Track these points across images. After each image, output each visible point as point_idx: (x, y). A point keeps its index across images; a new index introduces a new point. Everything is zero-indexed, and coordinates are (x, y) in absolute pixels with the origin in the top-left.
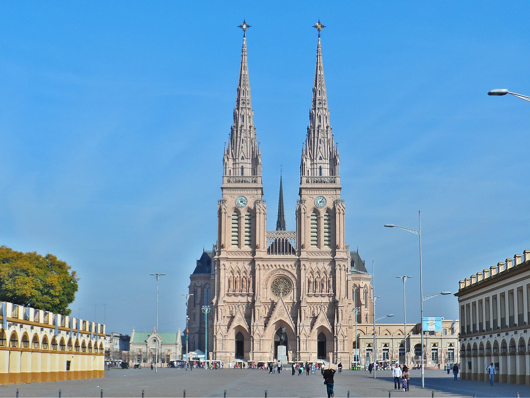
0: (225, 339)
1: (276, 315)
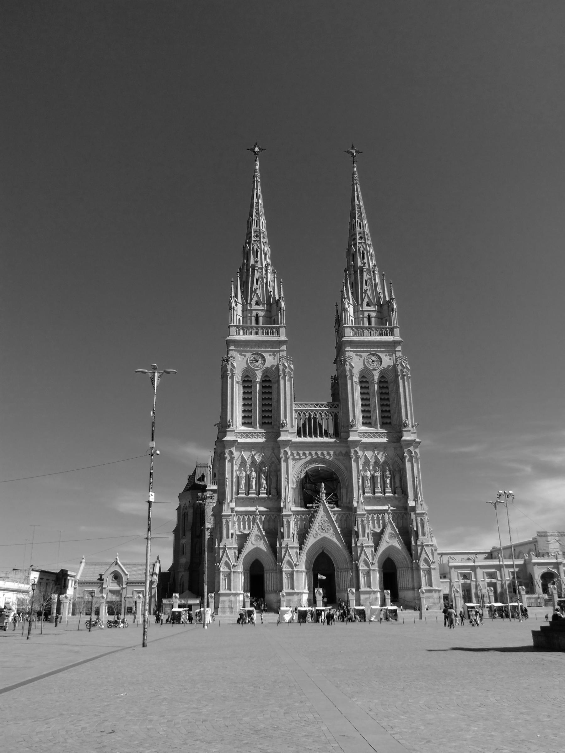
0: (234, 572)
1: (317, 530)
